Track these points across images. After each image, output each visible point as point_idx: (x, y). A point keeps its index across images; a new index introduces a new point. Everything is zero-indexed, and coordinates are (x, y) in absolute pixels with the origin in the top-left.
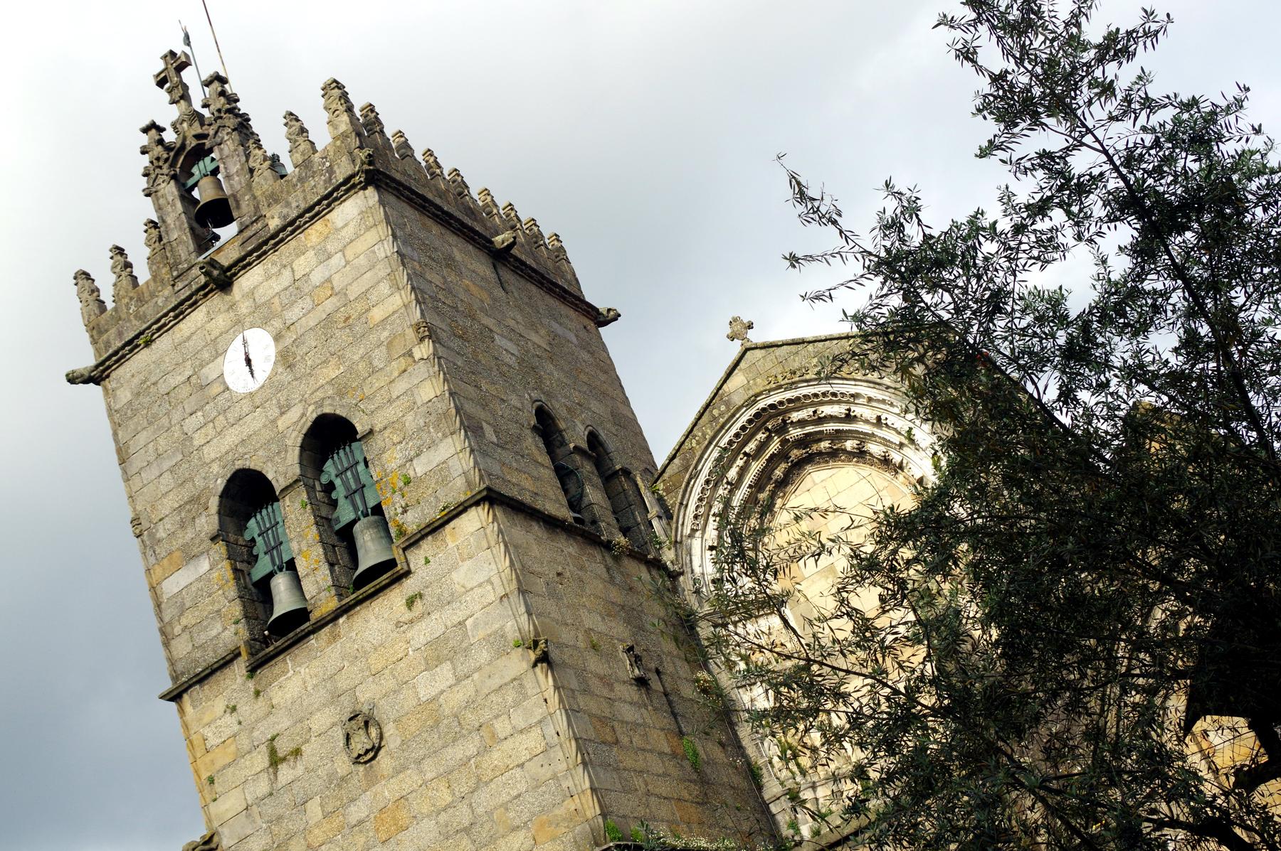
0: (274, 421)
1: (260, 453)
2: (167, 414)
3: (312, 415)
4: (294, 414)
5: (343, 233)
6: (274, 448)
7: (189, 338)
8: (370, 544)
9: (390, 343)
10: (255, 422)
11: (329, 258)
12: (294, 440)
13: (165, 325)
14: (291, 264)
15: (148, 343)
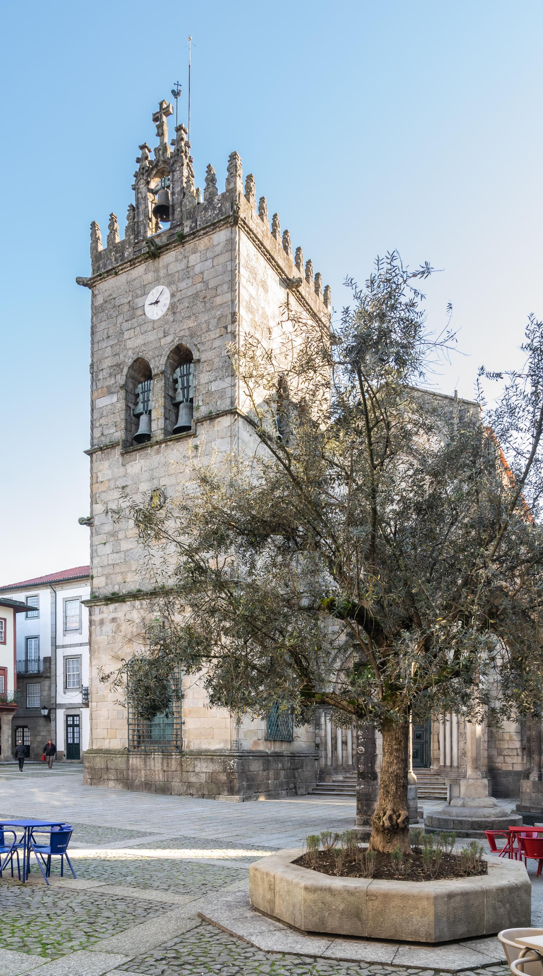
0: (160, 339)
1: (150, 353)
2: (117, 317)
3: (176, 343)
4: (169, 339)
5: (216, 249)
6: (157, 353)
7: (134, 280)
8: (184, 415)
9: (219, 319)
10: (152, 337)
11: (206, 260)
12: (166, 352)
13: (125, 268)
14: (188, 257)
15: (116, 274)
